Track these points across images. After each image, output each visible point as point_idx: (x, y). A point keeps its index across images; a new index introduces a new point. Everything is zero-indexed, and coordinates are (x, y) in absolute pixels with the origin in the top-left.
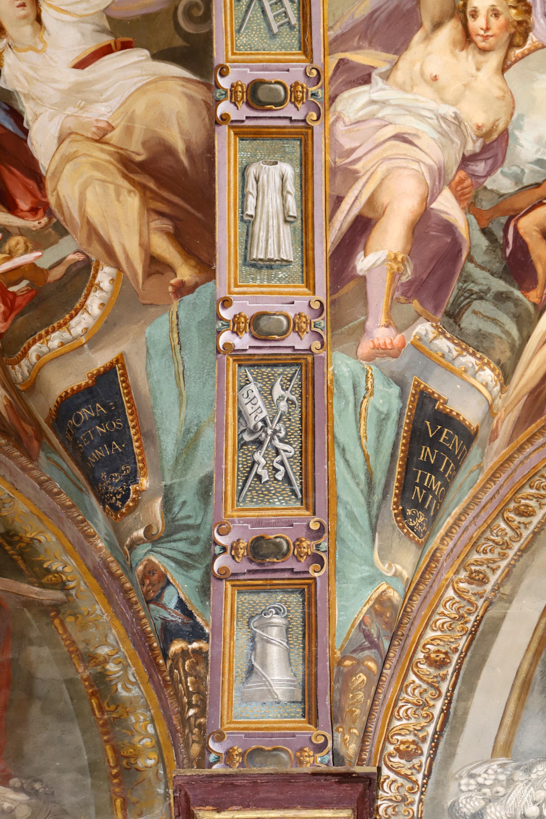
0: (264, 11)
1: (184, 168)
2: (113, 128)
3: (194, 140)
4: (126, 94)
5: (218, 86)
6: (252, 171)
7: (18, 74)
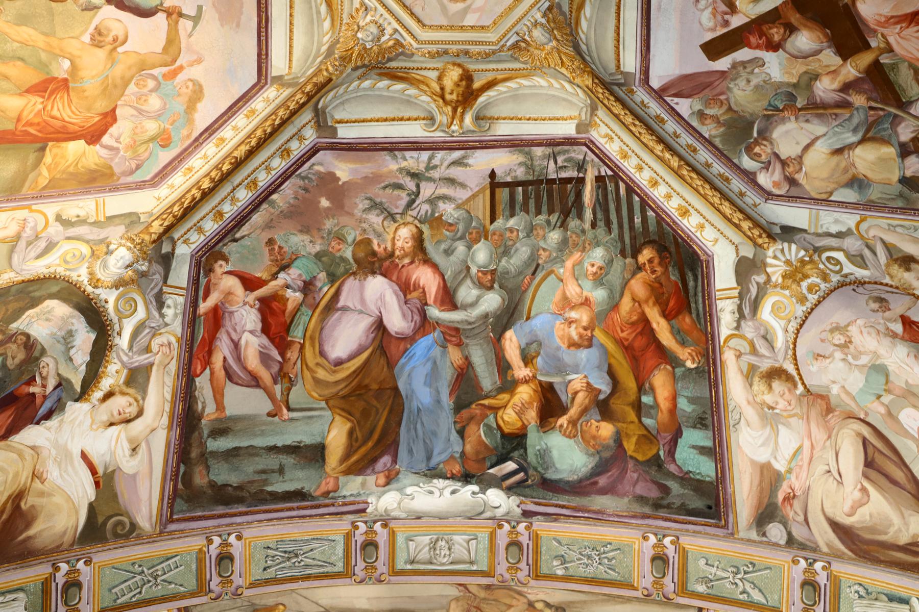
0: (125, 581)
1: (17, 538)
2: (42, 483)
3: (37, 540)
4: (66, 489)
5: (78, 560)
6: (21, 595)
7: (76, 413)
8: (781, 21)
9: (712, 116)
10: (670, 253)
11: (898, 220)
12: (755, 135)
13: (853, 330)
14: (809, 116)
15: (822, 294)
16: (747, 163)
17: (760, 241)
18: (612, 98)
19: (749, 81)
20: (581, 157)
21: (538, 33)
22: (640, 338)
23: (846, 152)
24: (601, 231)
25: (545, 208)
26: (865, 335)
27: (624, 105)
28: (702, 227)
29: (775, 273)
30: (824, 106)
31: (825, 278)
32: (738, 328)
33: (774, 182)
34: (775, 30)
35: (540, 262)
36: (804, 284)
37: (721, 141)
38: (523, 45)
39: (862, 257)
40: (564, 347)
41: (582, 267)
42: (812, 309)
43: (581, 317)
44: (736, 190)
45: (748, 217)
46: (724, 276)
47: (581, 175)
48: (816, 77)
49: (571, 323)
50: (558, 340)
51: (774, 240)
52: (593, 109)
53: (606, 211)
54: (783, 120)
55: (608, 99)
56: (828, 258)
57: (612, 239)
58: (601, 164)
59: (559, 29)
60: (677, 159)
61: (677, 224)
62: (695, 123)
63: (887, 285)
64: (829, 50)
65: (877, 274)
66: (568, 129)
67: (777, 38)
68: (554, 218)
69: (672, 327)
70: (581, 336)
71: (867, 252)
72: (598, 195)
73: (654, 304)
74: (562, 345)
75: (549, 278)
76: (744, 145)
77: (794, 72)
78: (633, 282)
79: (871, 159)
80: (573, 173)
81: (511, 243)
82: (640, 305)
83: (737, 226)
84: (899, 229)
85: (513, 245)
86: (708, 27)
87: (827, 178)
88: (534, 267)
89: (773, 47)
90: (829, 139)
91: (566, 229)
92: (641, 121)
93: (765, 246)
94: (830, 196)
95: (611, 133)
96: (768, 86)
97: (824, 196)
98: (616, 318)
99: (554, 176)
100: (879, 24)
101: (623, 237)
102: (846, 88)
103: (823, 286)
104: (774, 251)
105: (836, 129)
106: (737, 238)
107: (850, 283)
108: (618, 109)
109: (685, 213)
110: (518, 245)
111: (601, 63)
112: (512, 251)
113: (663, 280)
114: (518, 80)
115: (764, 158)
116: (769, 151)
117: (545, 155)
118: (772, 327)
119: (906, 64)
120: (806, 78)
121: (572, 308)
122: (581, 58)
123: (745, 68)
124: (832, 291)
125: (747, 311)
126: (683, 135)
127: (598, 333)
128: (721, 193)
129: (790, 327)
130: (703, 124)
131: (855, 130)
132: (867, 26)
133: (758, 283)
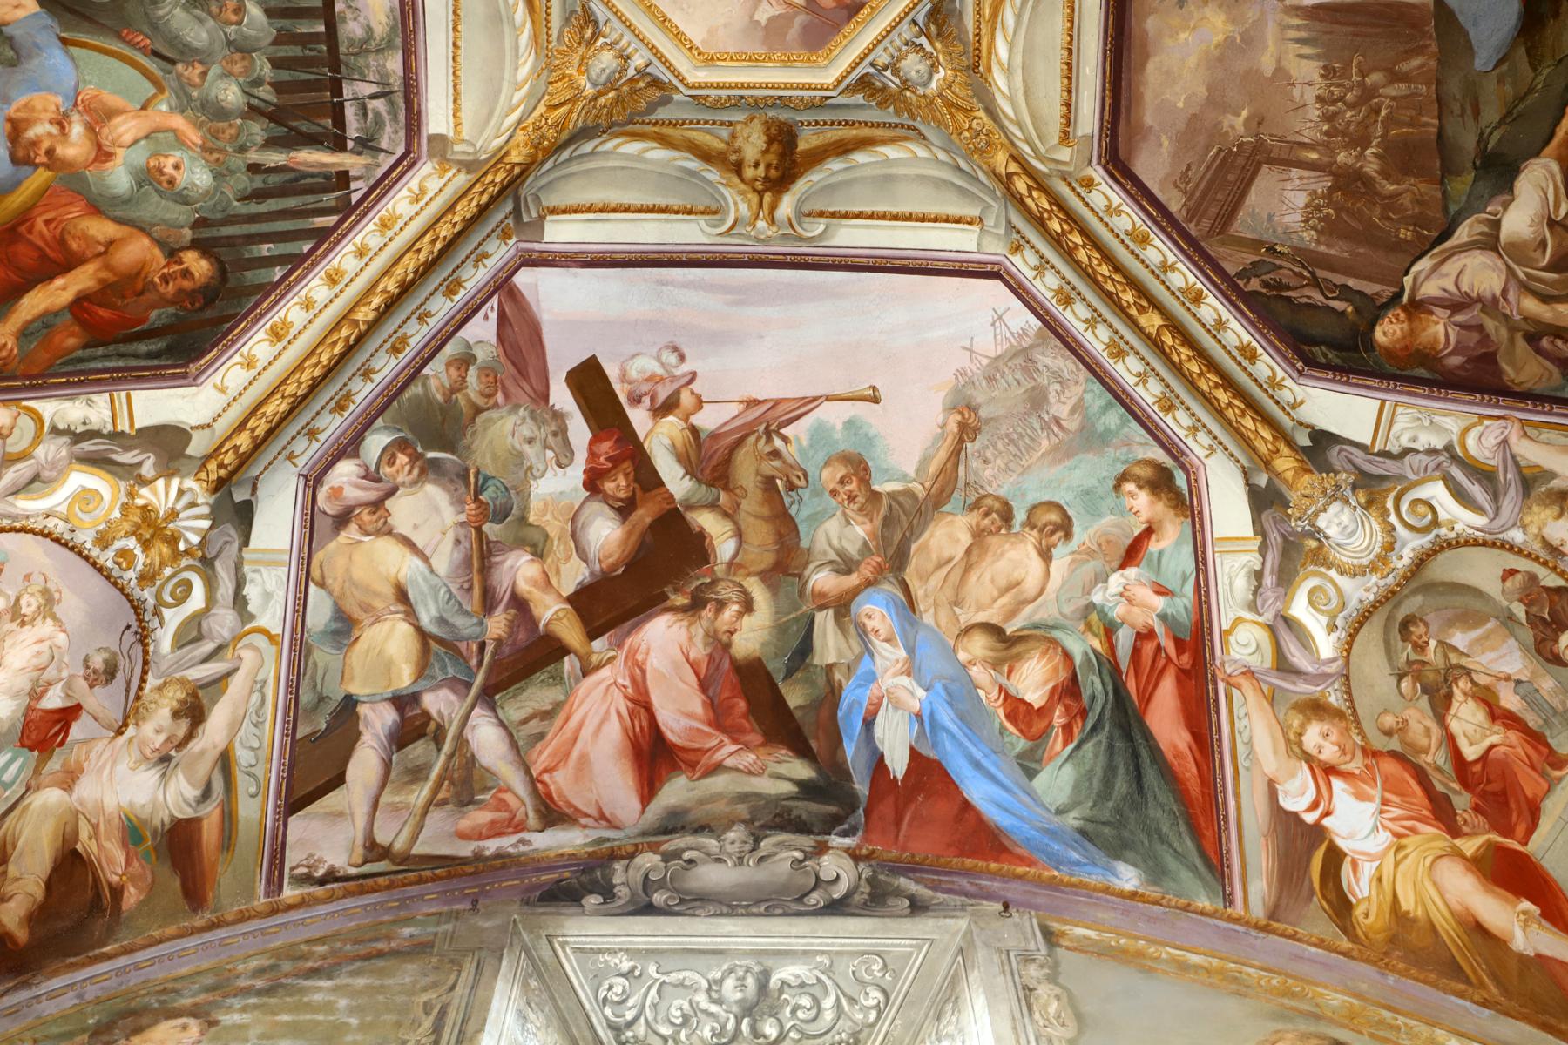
8: (638, 493)
9: (464, 379)
10: (201, 309)
11: (275, 695)
12: (430, 455)
13: (46, 628)
14: (467, 545)
15: (115, 573)
16: (376, 442)
17: (212, 466)
18: (485, 199)
19: (530, 441)
20: (384, 144)
21: (606, 61)
22: (35, 254)
23: (402, 608)
24: (244, 182)
25: (285, 75)
26: (36, 648)
27: (471, 223)
28: (249, 365)
29: (155, 493)
30: (486, 569)
31: (146, 578)
32: (55, 431)
33: (341, 489)
34: (623, 483)
35: (180, 67)
36: (131, 543)
37: (416, 396)
38: (588, 33)
39: (199, 638)
40: (11, 111)
41: (172, 147)
42: (87, 558)
43: (73, 145)
44: (320, 423)
45: (258, 445)
46: (155, 405)
47: (350, 144)
48: (539, 554)
49: (61, 125)
50: (23, 100)
51: (215, 490)
52: (468, 166)
53: (282, 192)
54: (458, 502)
55: (482, 193)
56: (188, 585)
57: (229, 201)
58: (372, 182)
59: (617, 101)
60: (371, 316)
61: (258, 320)
62: (449, 350)
63: (143, 680)
64: (587, 573)
65: (164, 666)
66: (437, 120)
67: (609, 486)
68: (266, 93)
69: (56, 314)
70: (35, 144)
71: (208, 647)
72: (312, 176)
73: (101, 281)
74: (14, 107)
75: (147, 84)
76: (410, 436)
77: (548, 517)
78: (146, 241)
79: (389, 650)
80: (353, 129)
81: (214, 9)
82: (100, 254)
83: (241, 427)
84: (256, 698)
85: (210, 13)
86: (627, 368)
87: (351, 579)
88: (169, 54)
89: (593, 482)
90: (425, 579)
91: (244, 116)
92: (442, 252)
93: (203, 475)
94: (317, 584)
95: (427, 198)
96: (521, 474)
97: (315, 573)
98: (74, 211)
99: (347, 92)
100: (632, 653)
101: (233, 223)
102: (520, 604)
103: (131, 575)
104: (191, 490)
105: (443, 590)
106: (222, 427)
107: (140, 621)
108: (465, 210)
109: (276, 334)
110: (211, 23)
111: (558, 179)
112: (197, 12)
113: (150, 297)
114: (528, 24)
115: (386, 470)
116: (400, 479)
117: (388, 75)
118: (54, 491)
119: (562, 698)
120: (537, 537)
121: (90, 128)
122: (558, 144)
123: (555, 434)
124: (122, 590)
125: (88, 446)
126: (425, 329)
127: (41, 177)
128: (305, 396)
129: (56, 521)
130: (448, 364)
131: (441, 621)
132: (629, 633)
133: (140, 464)
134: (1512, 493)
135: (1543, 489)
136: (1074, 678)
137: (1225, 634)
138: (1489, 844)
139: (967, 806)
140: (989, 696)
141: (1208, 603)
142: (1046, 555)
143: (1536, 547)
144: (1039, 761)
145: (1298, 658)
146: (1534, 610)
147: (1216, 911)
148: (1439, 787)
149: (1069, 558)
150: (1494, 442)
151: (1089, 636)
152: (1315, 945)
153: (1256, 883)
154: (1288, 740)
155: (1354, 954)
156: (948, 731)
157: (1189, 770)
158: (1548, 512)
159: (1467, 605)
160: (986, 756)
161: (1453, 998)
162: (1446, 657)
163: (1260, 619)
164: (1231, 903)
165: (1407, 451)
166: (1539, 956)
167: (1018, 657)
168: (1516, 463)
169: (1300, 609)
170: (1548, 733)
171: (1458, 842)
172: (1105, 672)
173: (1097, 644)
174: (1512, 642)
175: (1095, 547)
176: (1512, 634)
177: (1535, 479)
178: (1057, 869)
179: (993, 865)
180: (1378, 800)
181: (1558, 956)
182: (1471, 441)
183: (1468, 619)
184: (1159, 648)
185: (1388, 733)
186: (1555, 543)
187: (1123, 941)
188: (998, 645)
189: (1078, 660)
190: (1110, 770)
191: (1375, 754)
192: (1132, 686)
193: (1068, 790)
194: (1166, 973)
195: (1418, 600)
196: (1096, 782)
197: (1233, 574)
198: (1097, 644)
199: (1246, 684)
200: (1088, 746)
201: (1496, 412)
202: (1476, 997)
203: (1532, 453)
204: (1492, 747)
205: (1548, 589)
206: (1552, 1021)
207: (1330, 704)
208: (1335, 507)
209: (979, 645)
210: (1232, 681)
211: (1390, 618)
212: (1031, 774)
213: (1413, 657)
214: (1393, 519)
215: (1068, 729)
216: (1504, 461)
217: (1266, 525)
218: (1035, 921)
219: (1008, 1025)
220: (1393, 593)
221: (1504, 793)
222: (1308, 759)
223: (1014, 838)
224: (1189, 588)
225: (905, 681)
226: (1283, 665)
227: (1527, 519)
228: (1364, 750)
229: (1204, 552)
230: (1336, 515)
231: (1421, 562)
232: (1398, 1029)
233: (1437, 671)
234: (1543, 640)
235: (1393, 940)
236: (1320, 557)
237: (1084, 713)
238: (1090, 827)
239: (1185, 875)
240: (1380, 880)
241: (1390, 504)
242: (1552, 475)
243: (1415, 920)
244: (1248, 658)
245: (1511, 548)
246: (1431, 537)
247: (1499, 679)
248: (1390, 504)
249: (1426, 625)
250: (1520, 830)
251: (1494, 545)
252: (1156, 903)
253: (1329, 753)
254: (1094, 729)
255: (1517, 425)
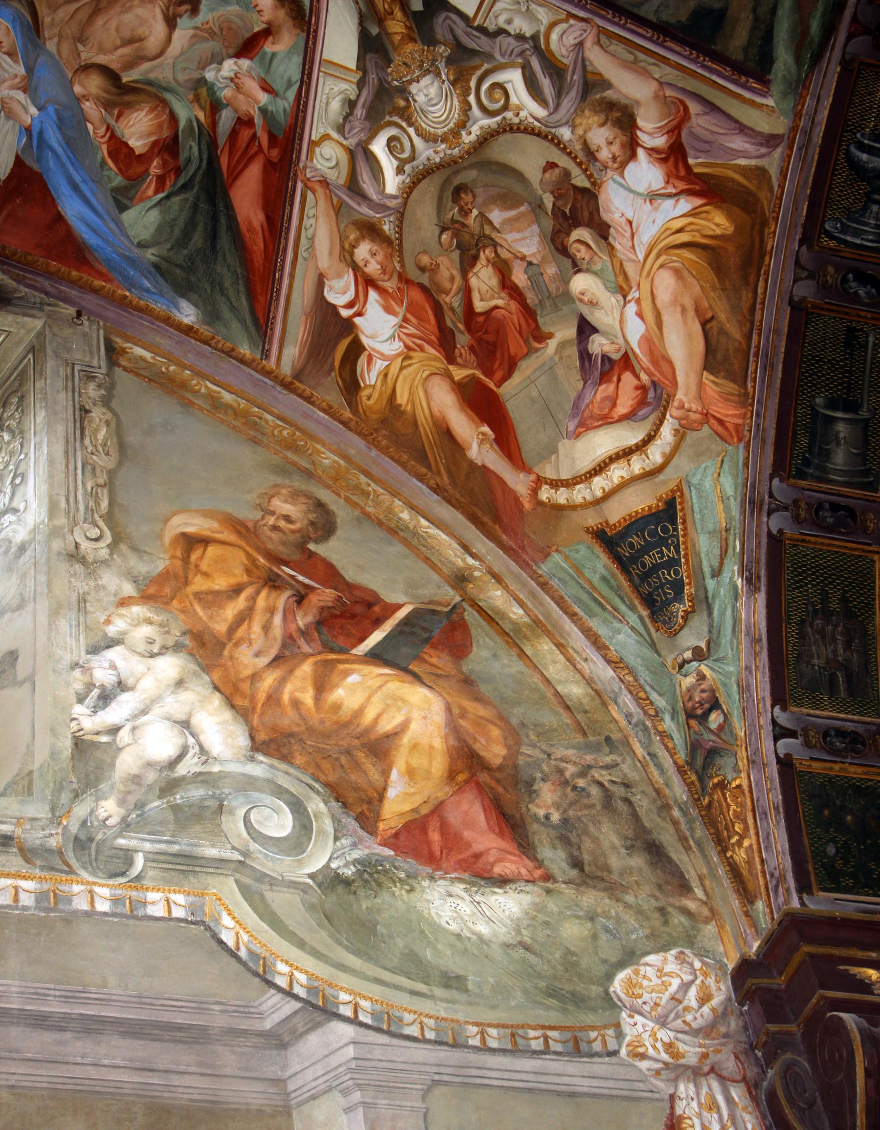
134: (573, 93)
135: (598, 97)
136: (175, 138)
137: (313, 144)
138: (473, 377)
139: (59, 218)
140: (95, 130)
141: (305, 112)
142: (171, 23)
143: (578, 147)
144: (131, 199)
145: (367, 185)
146: (560, 203)
147: (254, 360)
148: (449, 323)
149: (192, 32)
150: (573, 42)
151: (196, 106)
152: (324, 411)
153: (289, 355)
154: (342, 248)
155: (352, 424)
156: (54, 152)
157: (258, 245)
158: (596, 118)
159: (509, 186)
160: (84, 181)
161: (414, 480)
162: (482, 226)
163: (345, 142)
164: (268, 357)
165: (501, 32)
166: (484, 467)
167: (130, 106)
168: (584, 67)
169: (379, 147)
170: (539, 312)
171: (451, 368)
172: (204, 142)
173: (201, 116)
174: (535, 228)
175: (216, 30)
176: (537, 221)
177: (594, 86)
178: (129, 291)
179: (74, 273)
180: (401, 317)
181: (497, 472)
182: (554, 37)
183: (507, 200)
184: (255, 134)
185: (422, 269)
186: (593, 147)
187: (172, 368)
188: (113, 89)
189: (182, 124)
190: (191, 224)
191: (408, 282)
192: (224, 161)
193: (152, 230)
194: (201, 409)
195: (473, 174)
196: (177, 231)
197: (331, 96)
198: (201, 116)
199: (320, 191)
200: (176, 200)
201: (582, 14)
202: (432, 482)
203: (599, 60)
204: (496, 307)
205: (576, 188)
206: (479, 513)
207: (383, 231)
208: (426, 80)
209: (94, 84)
210: (310, 184)
211: (447, 181)
212: (122, 208)
213: (458, 218)
214: (472, 99)
215: (161, 181)
216: (576, 62)
217: (368, 65)
218: (101, 332)
219: (59, 448)
220: (455, 162)
221: (494, 345)
222: (356, 268)
223: (97, 256)
224: (291, 95)
225: (20, 96)
226: (353, 186)
227: (578, 121)
228: (400, 276)
229: (311, 68)
230: (426, 87)
231: (487, 138)
232: (368, 494)
233: (473, 235)
234: (559, 231)
235: (383, 421)
236: (406, 114)
237: (178, 171)
238: (164, 265)
239: (235, 325)
240: (386, 375)
241: (473, 84)
242: (606, 84)
243: (404, 413)
244: (328, 171)
245: (556, 142)
246: (498, 118)
247: (517, 257)
248: (473, 84)
249: (474, 196)
250: (499, 375)
251: (546, 137)
252: (206, 342)
253: (373, 268)
254: (184, 188)
255: (595, 31)
